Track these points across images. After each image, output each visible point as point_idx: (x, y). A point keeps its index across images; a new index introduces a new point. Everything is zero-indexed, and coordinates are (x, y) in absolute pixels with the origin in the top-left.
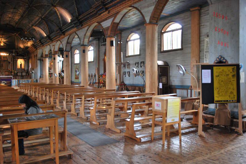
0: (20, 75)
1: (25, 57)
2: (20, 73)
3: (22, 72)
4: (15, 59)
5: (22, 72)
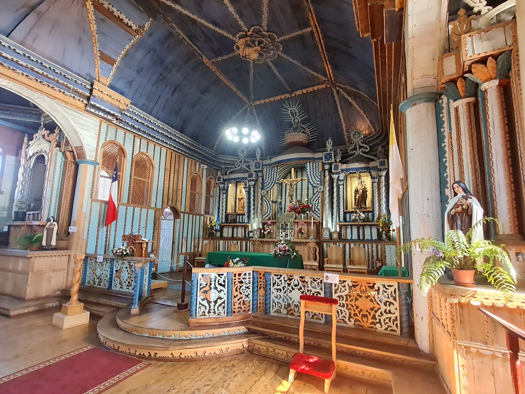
0: (355, 237)
1: (372, 164)
2: (355, 230)
3: (364, 226)
4: (335, 177)
5: (364, 226)
